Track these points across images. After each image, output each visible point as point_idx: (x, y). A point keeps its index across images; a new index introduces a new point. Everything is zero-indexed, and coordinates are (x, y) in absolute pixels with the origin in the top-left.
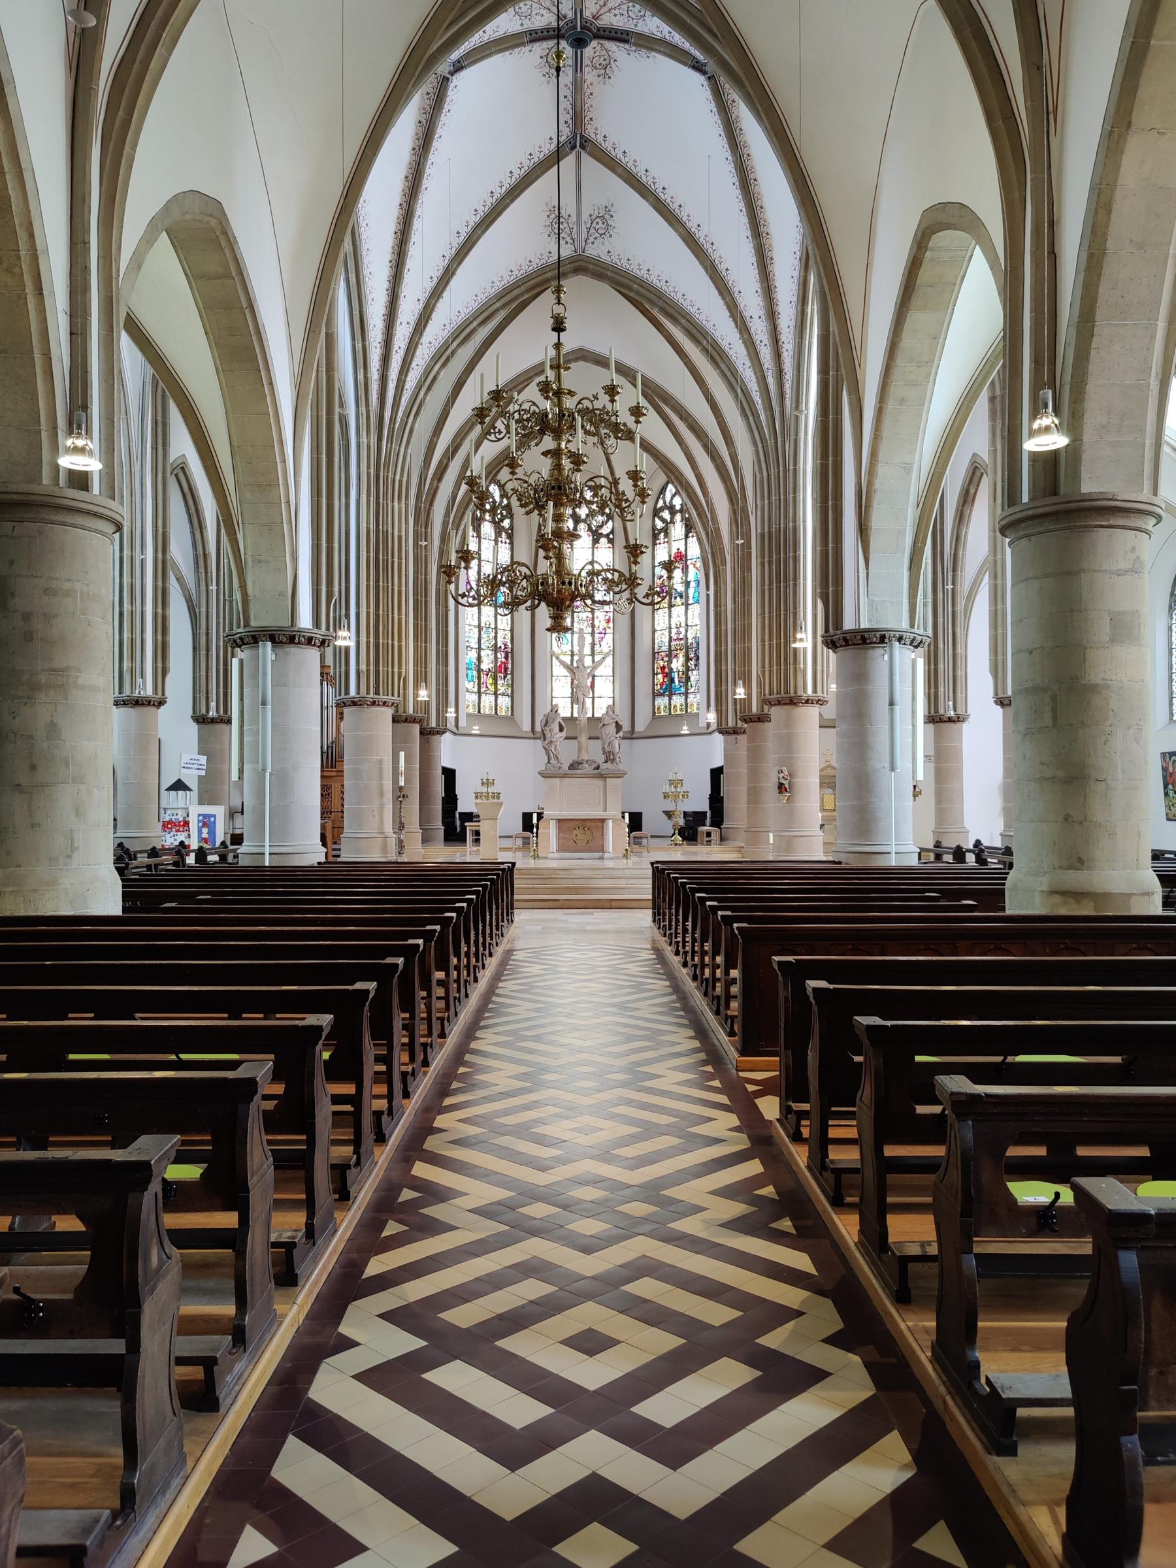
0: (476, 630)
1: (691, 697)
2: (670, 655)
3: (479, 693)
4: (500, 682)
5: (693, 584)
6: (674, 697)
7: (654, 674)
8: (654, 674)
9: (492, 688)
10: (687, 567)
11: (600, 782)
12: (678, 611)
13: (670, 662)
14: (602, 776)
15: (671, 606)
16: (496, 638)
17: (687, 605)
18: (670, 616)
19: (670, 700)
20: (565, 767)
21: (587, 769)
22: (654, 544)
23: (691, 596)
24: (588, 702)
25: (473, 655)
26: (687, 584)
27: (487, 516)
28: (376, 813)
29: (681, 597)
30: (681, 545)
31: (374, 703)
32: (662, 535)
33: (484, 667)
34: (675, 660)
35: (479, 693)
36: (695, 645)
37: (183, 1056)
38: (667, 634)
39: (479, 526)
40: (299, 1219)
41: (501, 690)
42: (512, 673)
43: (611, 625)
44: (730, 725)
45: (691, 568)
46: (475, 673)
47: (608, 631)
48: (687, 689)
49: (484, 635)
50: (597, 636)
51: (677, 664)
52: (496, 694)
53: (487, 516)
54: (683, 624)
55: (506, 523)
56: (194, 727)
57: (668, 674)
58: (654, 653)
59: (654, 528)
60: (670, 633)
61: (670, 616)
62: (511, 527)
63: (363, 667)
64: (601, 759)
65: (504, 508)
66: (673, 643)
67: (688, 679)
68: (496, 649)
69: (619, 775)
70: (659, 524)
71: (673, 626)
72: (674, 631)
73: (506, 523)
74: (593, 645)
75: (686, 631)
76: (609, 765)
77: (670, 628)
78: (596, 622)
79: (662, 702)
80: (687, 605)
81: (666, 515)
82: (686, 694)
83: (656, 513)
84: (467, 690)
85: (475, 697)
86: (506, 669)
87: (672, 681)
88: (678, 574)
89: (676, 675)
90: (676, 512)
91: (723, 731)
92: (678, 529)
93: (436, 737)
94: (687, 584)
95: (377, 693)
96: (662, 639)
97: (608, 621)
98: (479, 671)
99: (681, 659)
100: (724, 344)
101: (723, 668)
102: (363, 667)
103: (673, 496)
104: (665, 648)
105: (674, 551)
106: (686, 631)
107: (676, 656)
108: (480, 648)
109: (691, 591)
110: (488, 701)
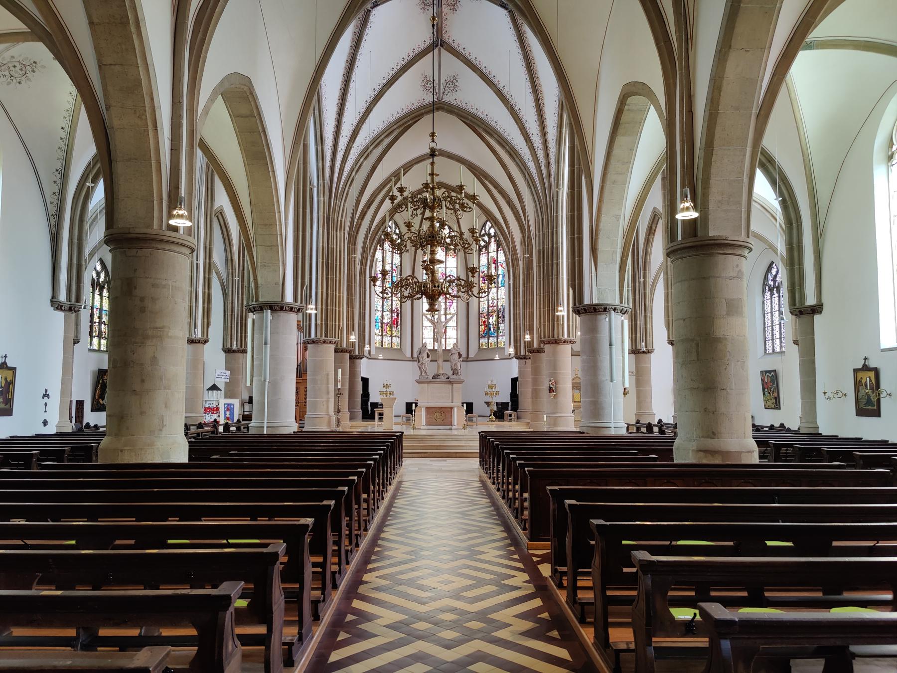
1: (500, 338)
2: (489, 315)
3: (382, 335)
4: (394, 329)
7: (480, 325)
8: (480, 325)
9: (389, 333)
11: (450, 386)
13: (488, 319)
14: (451, 383)
17: (498, 288)
20: (430, 377)
21: (443, 378)
22: (480, 254)
24: (443, 340)
25: (379, 314)
28: (325, 403)
30: (494, 255)
31: (324, 342)
33: (385, 321)
35: (382, 335)
37: (231, 541)
40: (294, 630)
41: (395, 334)
45: (500, 267)
51: (492, 320)
52: (391, 336)
56: (224, 354)
57: (487, 326)
63: (319, 322)
64: (450, 373)
65: (397, 234)
67: (498, 328)
68: (392, 311)
69: (461, 382)
74: (446, 309)
79: (484, 341)
80: (498, 288)
81: (486, 238)
82: (497, 337)
85: (380, 338)
87: (490, 329)
91: (518, 357)
92: (493, 246)
93: (358, 361)
95: (326, 336)
96: (484, 306)
98: (382, 323)
99: (495, 317)
100: (518, 148)
102: (319, 322)
104: (486, 311)
108: (383, 311)
110: (387, 340)
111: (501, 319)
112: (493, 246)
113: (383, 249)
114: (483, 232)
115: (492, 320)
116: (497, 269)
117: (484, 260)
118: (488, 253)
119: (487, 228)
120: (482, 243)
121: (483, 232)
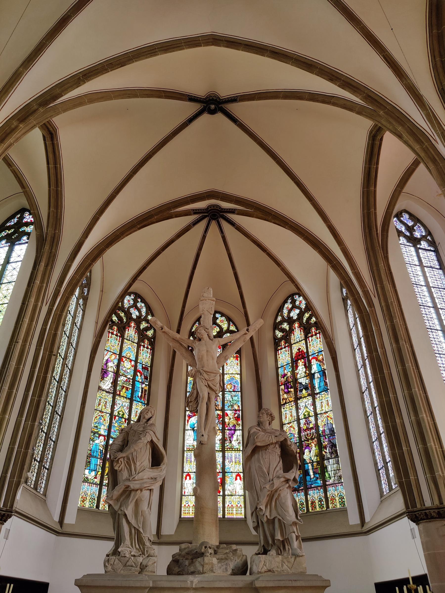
0: (107, 418)
1: (331, 491)
5: (317, 375)
6: (311, 492)
10: (310, 362)
12: (305, 403)
15: (297, 399)
17: (313, 395)
18: (297, 409)
19: (306, 495)
22: (276, 350)
23: (317, 386)
24: (220, 499)
26: (311, 376)
27: (133, 324)
29: (306, 388)
32: (283, 343)
34: (307, 451)
36: (327, 432)
38: (295, 425)
39: (124, 329)
43: (240, 422)
44: (428, 504)
45: (314, 362)
46: (99, 462)
47: (237, 428)
48: (324, 481)
49: (115, 425)
50: (227, 432)
51: (310, 455)
53: (133, 324)
54: (312, 413)
55: (150, 333)
59: (275, 338)
60: (299, 424)
61: (297, 409)
62: (154, 336)
66: (303, 434)
67: (324, 469)
70: (279, 334)
71: (301, 416)
72: (302, 422)
73: (150, 333)
74: (223, 440)
75: (316, 420)
76: (273, 560)
77: (298, 420)
78: (227, 420)
80: (313, 395)
81: (285, 326)
82: (325, 487)
83: (276, 326)
84: (86, 480)
87: (306, 473)
88: (301, 369)
89: (310, 467)
90: (295, 321)
91: (416, 517)
92: (298, 334)
94: (311, 376)
97: (237, 419)
99: (314, 449)
101: (398, 421)
103: (290, 311)
105: (295, 351)
106: (316, 420)
107: (308, 446)
109: (316, 382)
111: (327, 452)
112: (298, 334)
113: (122, 336)
114: (279, 318)
115: (310, 455)
116: (308, 366)
117: (284, 357)
118: (290, 346)
119: (285, 311)
120: (279, 334)
121: (279, 318)
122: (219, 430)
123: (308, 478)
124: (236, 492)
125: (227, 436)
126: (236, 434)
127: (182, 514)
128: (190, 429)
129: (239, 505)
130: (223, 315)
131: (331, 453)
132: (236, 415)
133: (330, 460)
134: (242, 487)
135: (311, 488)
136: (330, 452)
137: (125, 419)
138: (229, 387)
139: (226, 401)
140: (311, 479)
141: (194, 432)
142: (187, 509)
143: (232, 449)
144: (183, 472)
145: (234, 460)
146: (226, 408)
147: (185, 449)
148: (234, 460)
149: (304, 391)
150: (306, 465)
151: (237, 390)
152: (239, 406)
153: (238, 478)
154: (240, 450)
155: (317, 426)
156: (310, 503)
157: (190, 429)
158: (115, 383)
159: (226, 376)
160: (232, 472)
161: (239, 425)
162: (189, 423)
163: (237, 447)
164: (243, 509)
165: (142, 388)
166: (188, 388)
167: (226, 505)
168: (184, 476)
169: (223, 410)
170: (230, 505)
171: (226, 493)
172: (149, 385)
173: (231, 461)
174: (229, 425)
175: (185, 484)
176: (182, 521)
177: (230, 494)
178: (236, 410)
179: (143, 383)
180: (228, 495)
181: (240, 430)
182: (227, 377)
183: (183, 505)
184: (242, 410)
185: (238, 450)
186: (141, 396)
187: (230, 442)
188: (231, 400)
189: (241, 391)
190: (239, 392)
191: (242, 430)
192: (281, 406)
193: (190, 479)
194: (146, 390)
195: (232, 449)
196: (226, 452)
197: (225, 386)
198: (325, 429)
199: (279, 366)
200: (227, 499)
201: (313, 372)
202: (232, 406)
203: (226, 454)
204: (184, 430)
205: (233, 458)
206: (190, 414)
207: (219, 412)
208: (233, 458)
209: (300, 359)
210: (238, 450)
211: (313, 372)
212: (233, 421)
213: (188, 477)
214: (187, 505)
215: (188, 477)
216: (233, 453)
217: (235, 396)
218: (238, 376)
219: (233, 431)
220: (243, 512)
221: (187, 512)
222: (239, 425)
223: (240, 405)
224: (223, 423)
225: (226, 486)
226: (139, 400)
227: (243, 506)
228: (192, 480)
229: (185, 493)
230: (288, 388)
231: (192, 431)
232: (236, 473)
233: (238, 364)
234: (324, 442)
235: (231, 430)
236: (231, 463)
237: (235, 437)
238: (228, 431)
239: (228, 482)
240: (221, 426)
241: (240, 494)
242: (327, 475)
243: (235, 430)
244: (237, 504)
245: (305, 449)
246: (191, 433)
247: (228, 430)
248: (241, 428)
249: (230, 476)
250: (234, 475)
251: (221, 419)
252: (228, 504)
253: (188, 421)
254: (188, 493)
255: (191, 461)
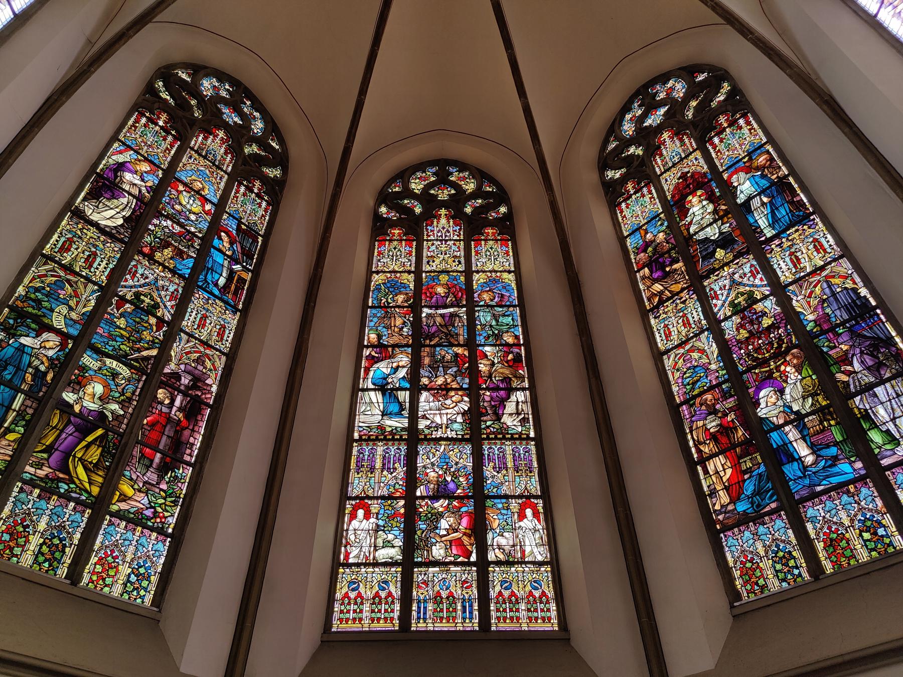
2: (739, 388)
6: (814, 511)
7: (693, 465)
16: (165, 346)
18: (705, 300)
19: (798, 524)
42: (199, 466)
47: (514, 385)
57: (753, 440)
58: (674, 408)
61: (705, 300)
68: (152, 374)
78: (483, 367)
86: (178, 445)
106: (784, 301)
122: (461, 389)
123: (791, 470)
124: (523, 552)
125: (486, 404)
126: (513, 398)
127: (335, 622)
128: (371, 386)
129: (537, 594)
130: (462, 166)
131: (875, 369)
132: (510, 357)
133: (879, 390)
134: (545, 538)
135: (814, 496)
136: (868, 368)
137: (161, 321)
138: (486, 296)
139: (479, 327)
140: (805, 468)
141: (384, 395)
142: (352, 607)
143: (503, 435)
144: (344, 497)
145: (510, 464)
146: (480, 339)
147: (356, 436)
148: (510, 464)
149: (720, 254)
150: (774, 435)
151: (508, 303)
152: (517, 337)
153: (529, 512)
154: (528, 438)
155: (790, 316)
156: (820, 546)
157: (371, 386)
158: (136, 222)
159: (476, 277)
160: (506, 497)
161: (522, 378)
162: (371, 374)
163: (520, 429)
164: (553, 606)
165: (232, 273)
166: (370, 300)
167: (493, 594)
168: (349, 507)
169: (471, 344)
170: (506, 593)
171: (491, 557)
172: (256, 273)
173: (502, 467)
174: (490, 376)
175: (350, 533)
176: (331, 642)
177: (502, 557)
178: (507, 345)
179: (234, 260)
180: (499, 563)
181: (523, 389)
182: (478, 279)
183: (338, 595)
184: (527, 344)
185: (521, 438)
186: (227, 286)
187: (494, 418)
188: (494, 323)
189: (522, 305)
190: (515, 306)
191: (532, 388)
192: (644, 314)
193: (367, 516)
194: (242, 281)
195: (503, 435)
196: (486, 442)
197: (476, 295)
198: (828, 311)
199: (626, 234)
200: (496, 574)
201: (741, 198)
202: (498, 336)
203: (486, 447)
204: (356, 390)
205: (509, 458)
206: (373, 353)
207: (460, 351)
208: (509, 458)
209: (693, 193)
210: (521, 438)
211: (741, 198)
212: (502, 370)
213: (361, 513)
214: (352, 595)
215: (361, 513)
216: (508, 448)
217: (504, 315)
218: (509, 278)
219: (502, 392)
220: (554, 614)
221: (351, 615)
222: (522, 378)
223: (519, 331)
224: (474, 373)
225: (490, 536)
226: (216, 292)
227: (550, 593)
228: (372, 520)
229: (347, 555)
230: (662, 267)
231: (380, 396)
232: (520, 497)
233: (507, 253)
234: (832, 348)
235: (497, 389)
236: (504, 472)
237: (510, 407)
238: (488, 393)
239: (495, 525)
240: (467, 380)
241: (540, 558)
242: (875, 437)
243: (510, 390)
244: (528, 588)
245: (759, 389)
246: (375, 397)
247: (487, 389)
248: (526, 384)
249: (500, 506)
250: (514, 505)
251: (467, 365)
252: (498, 588)
253: (367, 370)
254: (358, 556)
255: (372, 469)
